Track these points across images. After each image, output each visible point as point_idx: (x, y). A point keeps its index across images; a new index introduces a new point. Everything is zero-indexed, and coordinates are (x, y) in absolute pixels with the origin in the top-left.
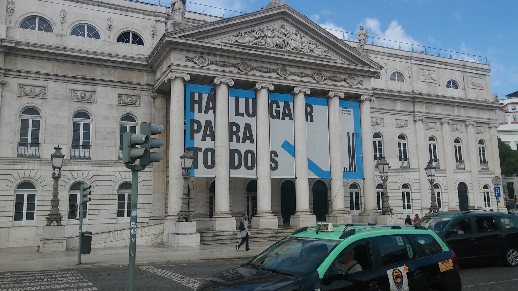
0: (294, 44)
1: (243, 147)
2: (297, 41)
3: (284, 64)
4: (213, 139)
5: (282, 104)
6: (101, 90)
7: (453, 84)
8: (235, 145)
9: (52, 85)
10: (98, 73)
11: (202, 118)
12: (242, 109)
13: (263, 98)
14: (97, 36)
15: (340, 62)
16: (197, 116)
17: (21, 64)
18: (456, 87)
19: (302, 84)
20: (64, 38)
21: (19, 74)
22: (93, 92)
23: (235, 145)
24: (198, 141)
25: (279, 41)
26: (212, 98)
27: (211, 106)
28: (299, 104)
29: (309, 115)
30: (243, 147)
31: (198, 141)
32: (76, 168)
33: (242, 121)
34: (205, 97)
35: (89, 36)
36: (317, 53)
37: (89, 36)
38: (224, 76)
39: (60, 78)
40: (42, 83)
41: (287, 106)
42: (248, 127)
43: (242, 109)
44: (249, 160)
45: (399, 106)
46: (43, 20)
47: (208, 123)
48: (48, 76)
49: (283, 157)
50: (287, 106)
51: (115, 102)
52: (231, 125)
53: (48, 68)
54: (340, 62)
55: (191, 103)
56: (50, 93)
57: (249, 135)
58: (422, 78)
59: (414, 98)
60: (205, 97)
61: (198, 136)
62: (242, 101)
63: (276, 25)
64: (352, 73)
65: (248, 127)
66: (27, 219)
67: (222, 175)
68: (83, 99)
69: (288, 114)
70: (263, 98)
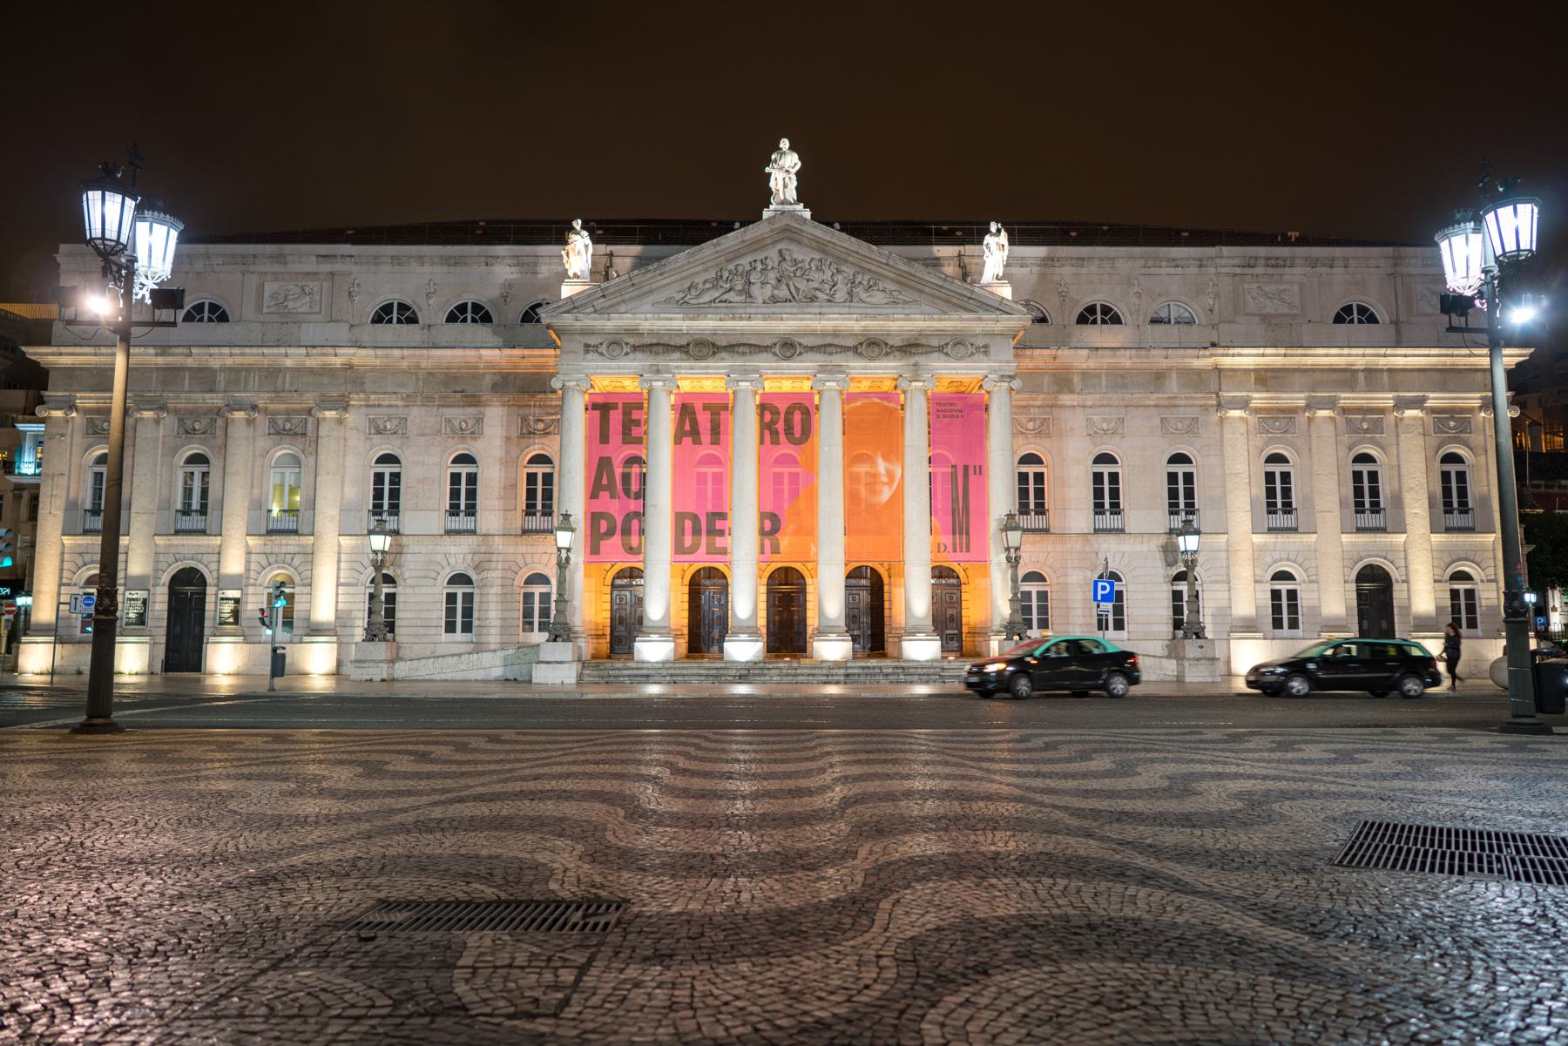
18: (1372, 319)
20: (433, 331)
22: (479, 421)
32: (453, 550)
35: (474, 321)
37: (474, 321)
40: (401, 412)
46: (403, 307)
51: (515, 433)
56: (412, 428)
63: (772, 254)
66: (463, 631)
68: (462, 433)
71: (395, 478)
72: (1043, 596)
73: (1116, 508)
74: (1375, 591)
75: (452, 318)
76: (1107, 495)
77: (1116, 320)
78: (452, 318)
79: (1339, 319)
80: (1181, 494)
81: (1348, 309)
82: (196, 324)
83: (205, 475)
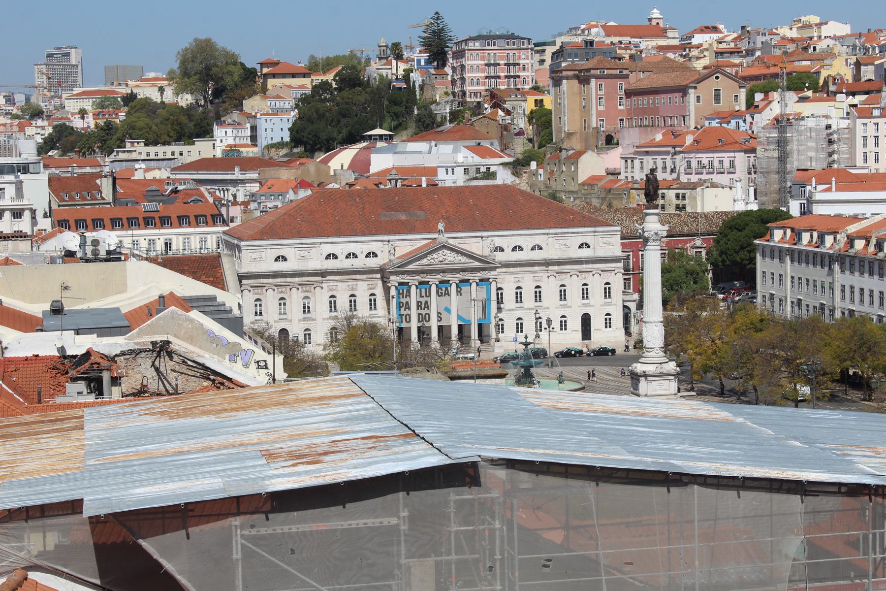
0: (449, 259)
1: (424, 312)
2: (450, 257)
3: (444, 271)
4: (409, 309)
5: (444, 289)
6: (359, 283)
7: (584, 245)
8: (420, 311)
9: (339, 284)
10: (358, 277)
11: (404, 300)
12: (423, 294)
13: (434, 289)
14: (356, 257)
15: (477, 264)
16: (402, 300)
17: (328, 278)
18: (589, 247)
19: (454, 278)
21: (327, 281)
23: (420, 311)
24: (403, 311)
25: (441, 259)
26: (409, 291)
27: (409, 294)
28: (453, 289)
29: (459, 292)
30: (424, 312)
31: (403, 311)
33: (423, 300)
34: (405, 291)
36: (463, 261)
38: (413, 280)
39: (342, 280)
41: (446, 289)
42: (426, 302)
43: (423, 294)
44: (426, 318)
45: (536, 268)
46: (334, 255)
47: (407, 303)
48: (337, 280)
49: (444, 315)
50: (446, 289)
52: (418, 302)
53: (337, 277)
54: (477, 264)
55: (399, 294)
57: (427, 306)
58: (557, 246)
59: (547, 263)
60: (405, 291)
61: (402, 309)
62: (423, 290)
64: (484, 269)
65: (426, 302)
67: (414, 326)
68: (353, 289)
69: (448, 293)
70: (434, 289)
71: (335, 302)
72: (502, 325)
73: (521, 301)
74: (586, 320)
75: (347, 257)
76: (519, 298)
77: (522, 250)
78: (347, 257)
79: (580, 247)
80: (538, 296)
81: (582, 244)
82: (277, 263)
83: (285, 304)
